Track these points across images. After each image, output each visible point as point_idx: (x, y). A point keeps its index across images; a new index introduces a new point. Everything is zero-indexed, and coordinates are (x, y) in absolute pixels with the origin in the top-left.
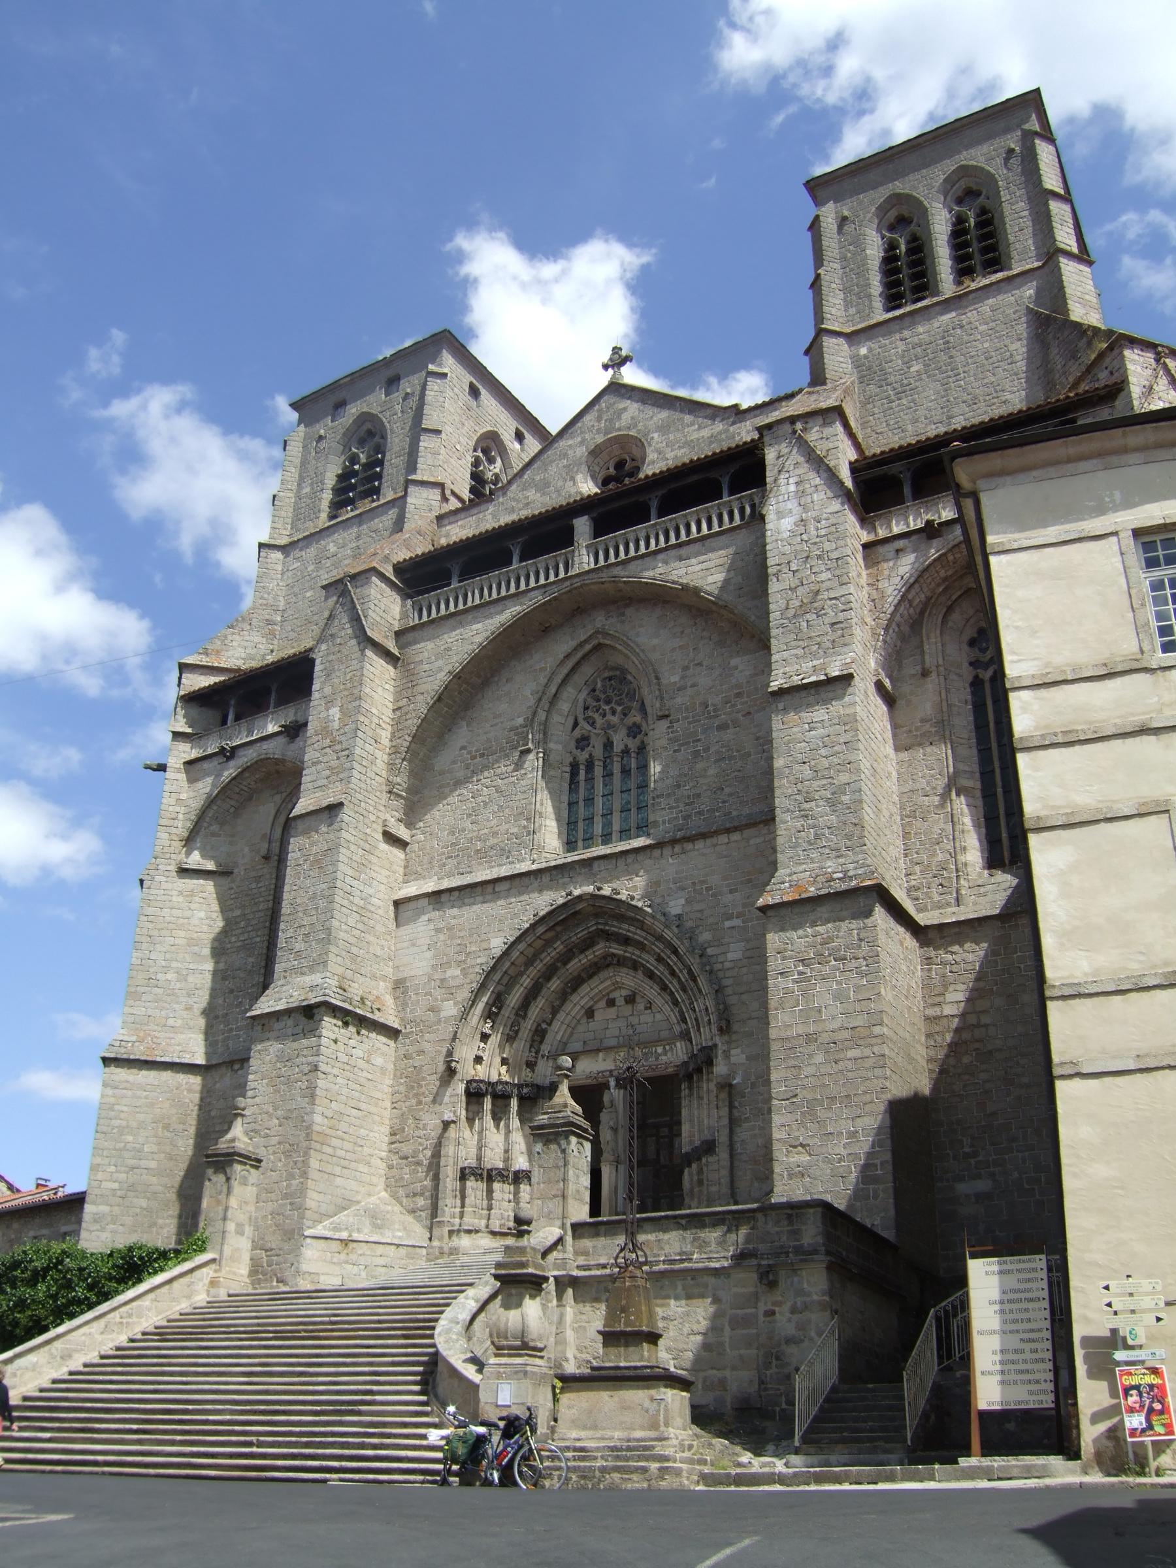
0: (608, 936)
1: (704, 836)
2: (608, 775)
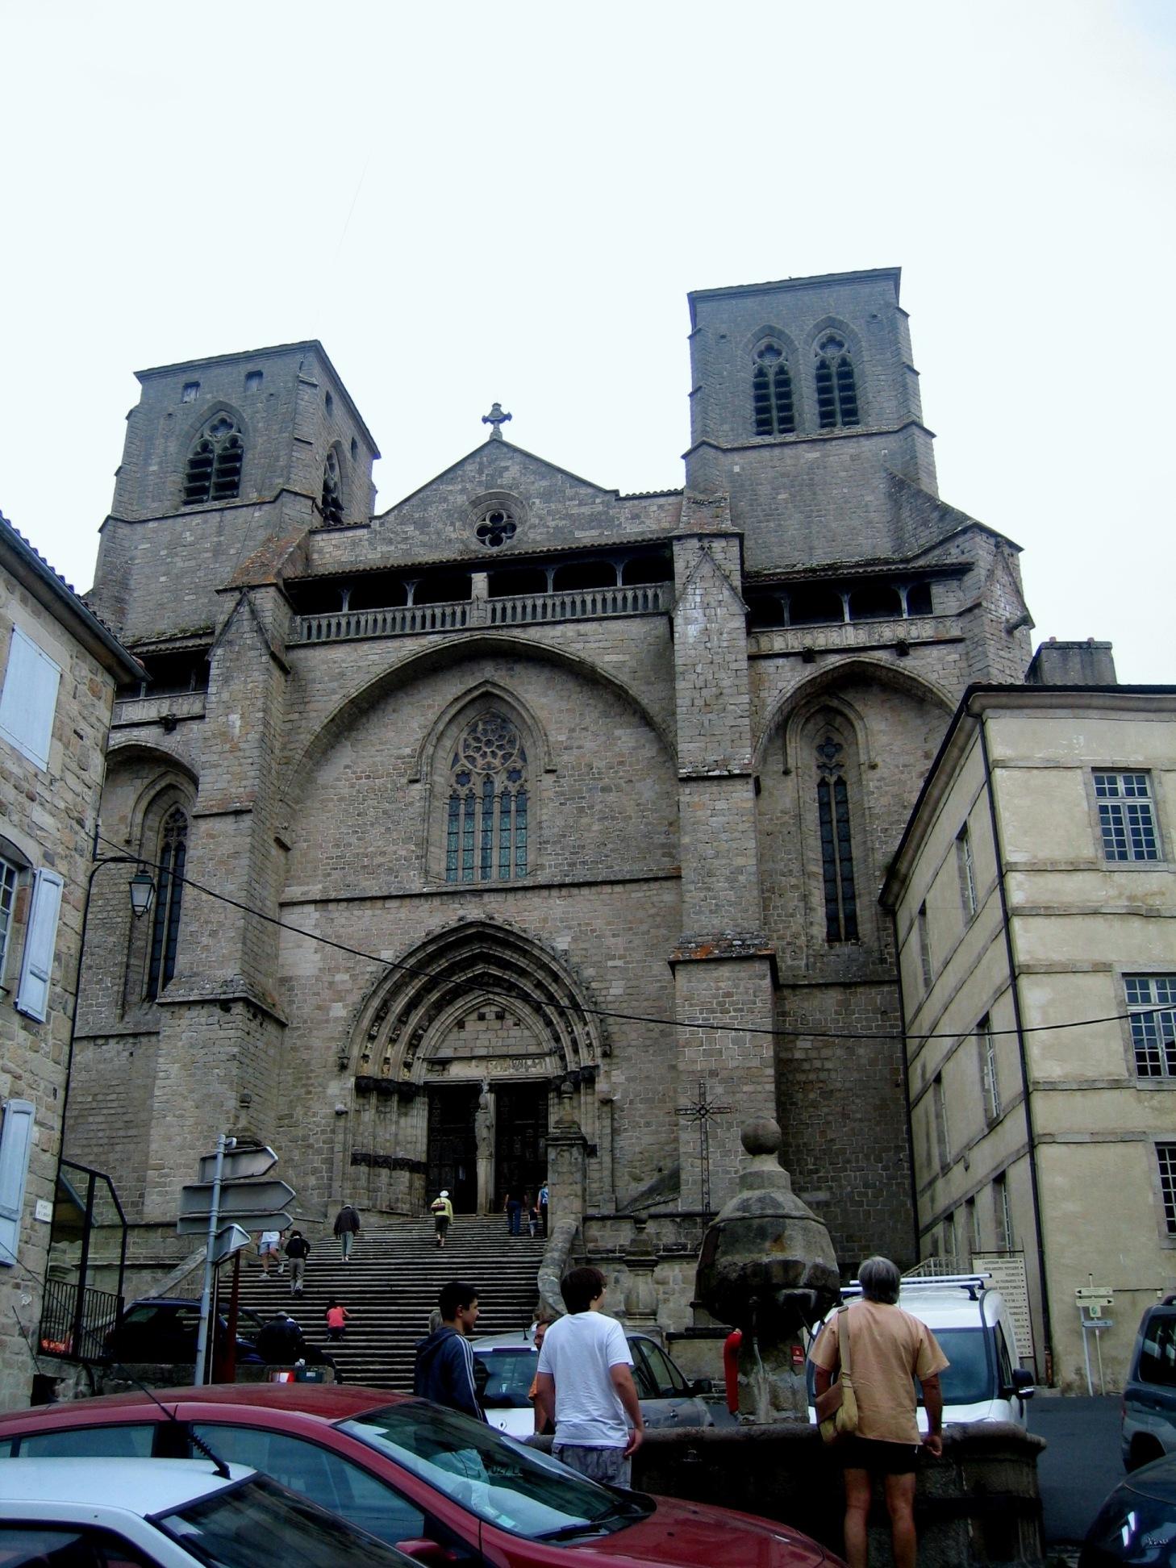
2: (488, 814)
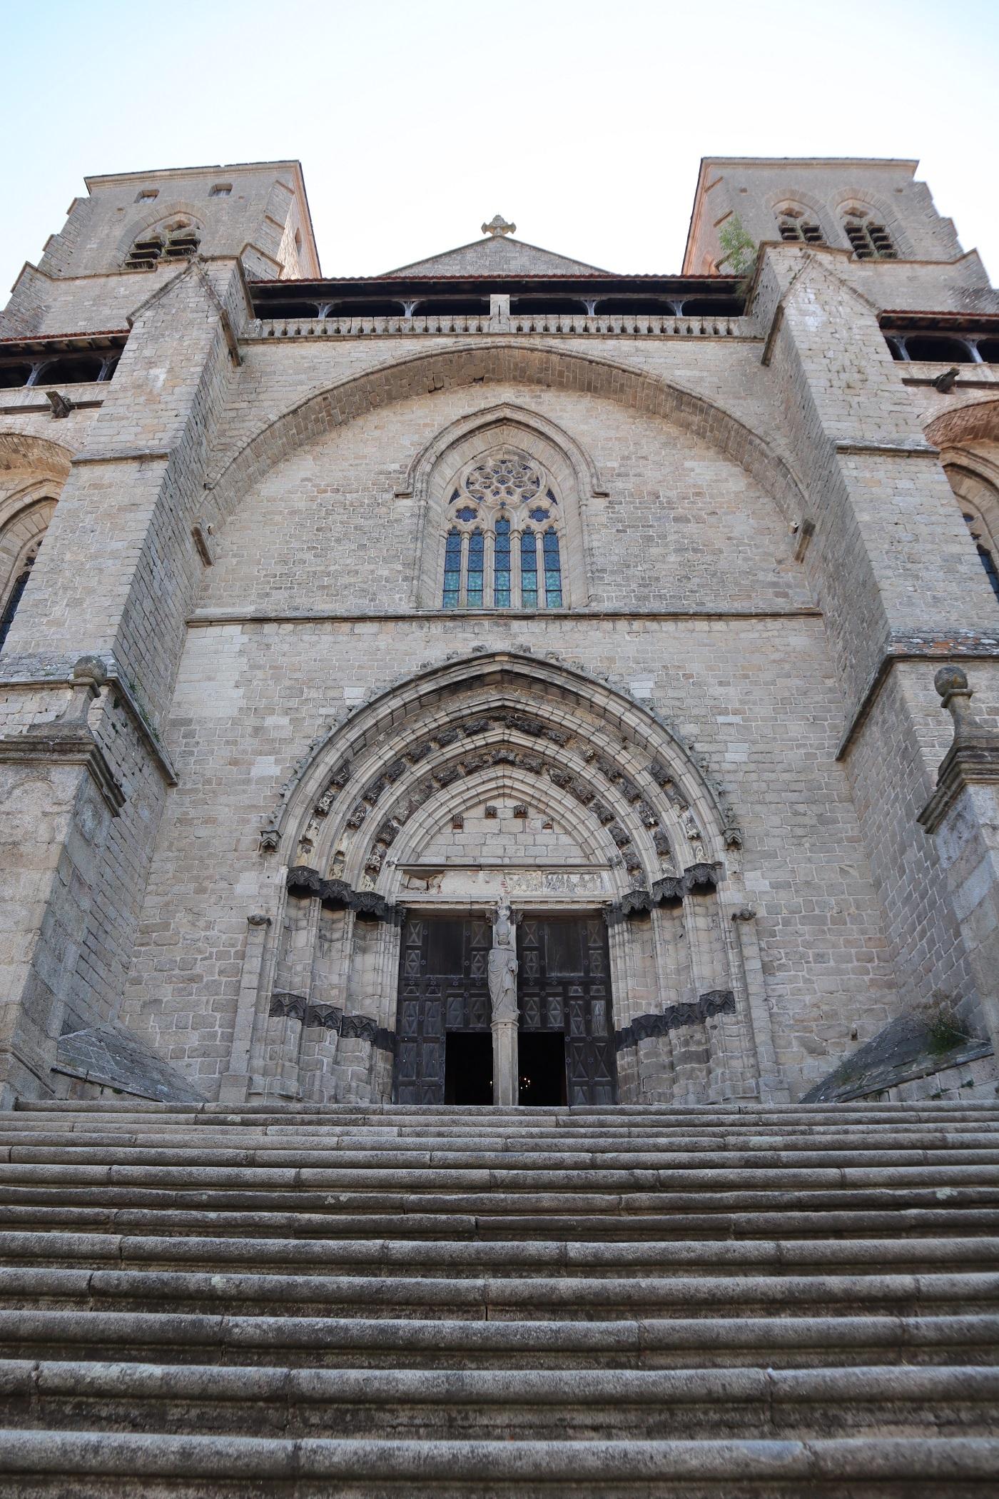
1: (675, 616)
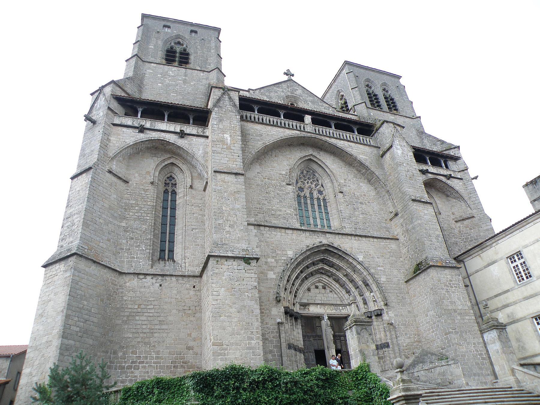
0: (322, 261)
